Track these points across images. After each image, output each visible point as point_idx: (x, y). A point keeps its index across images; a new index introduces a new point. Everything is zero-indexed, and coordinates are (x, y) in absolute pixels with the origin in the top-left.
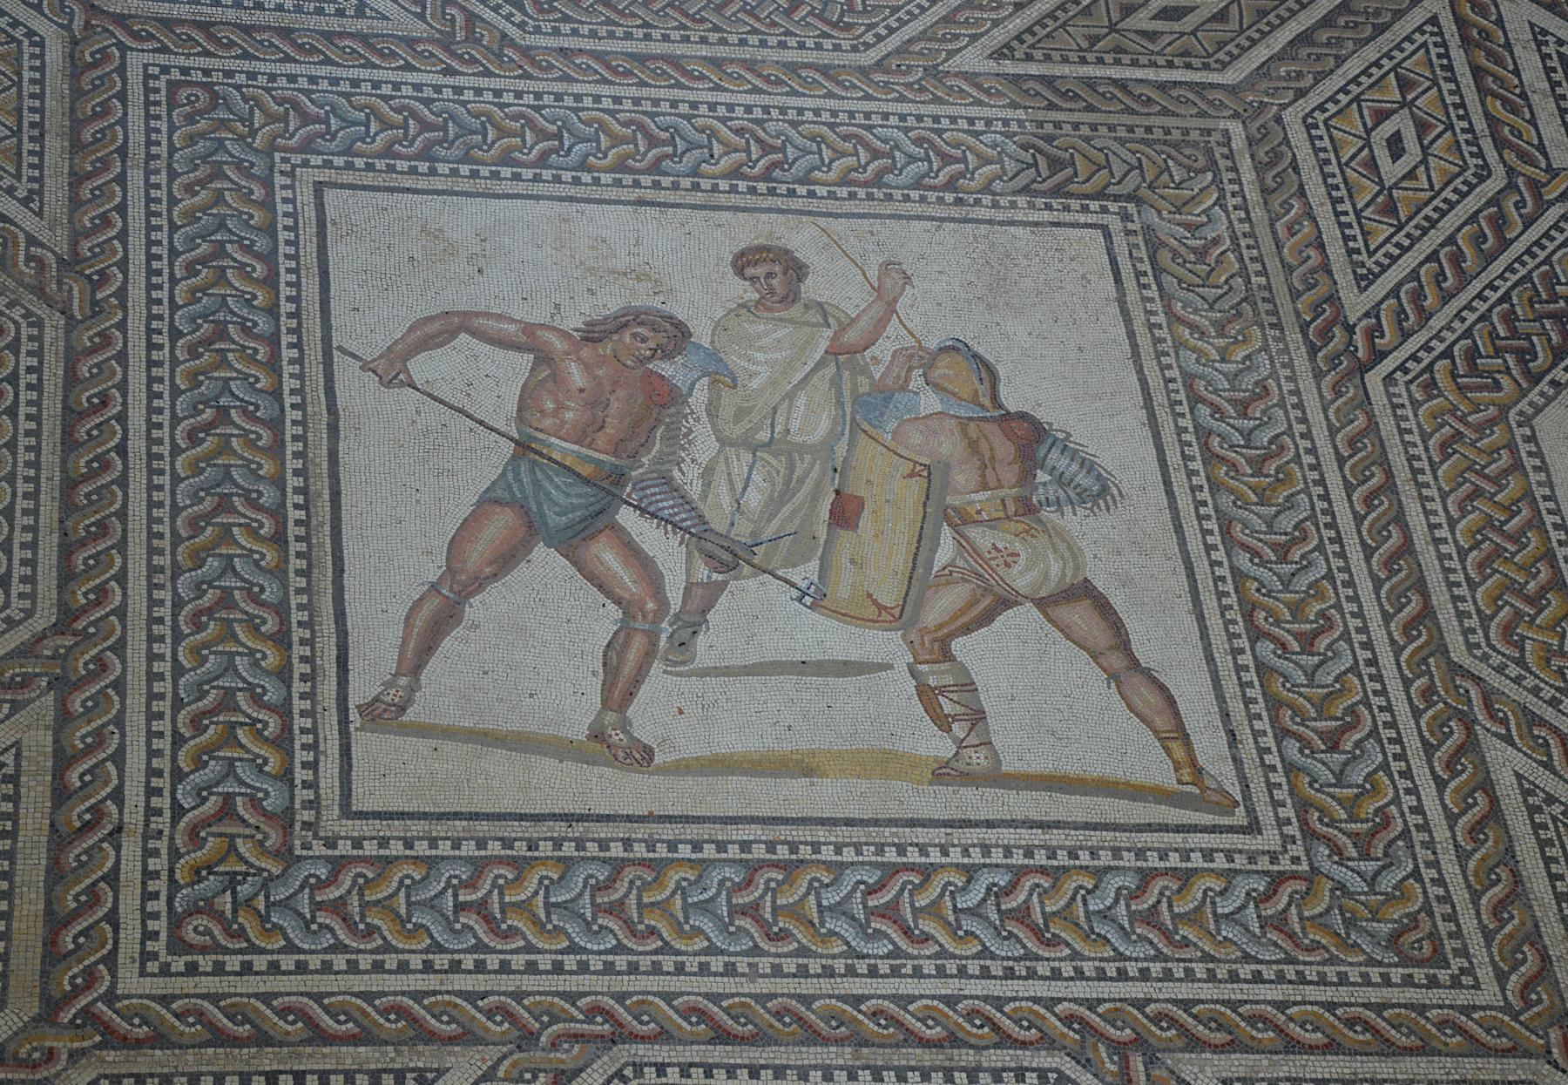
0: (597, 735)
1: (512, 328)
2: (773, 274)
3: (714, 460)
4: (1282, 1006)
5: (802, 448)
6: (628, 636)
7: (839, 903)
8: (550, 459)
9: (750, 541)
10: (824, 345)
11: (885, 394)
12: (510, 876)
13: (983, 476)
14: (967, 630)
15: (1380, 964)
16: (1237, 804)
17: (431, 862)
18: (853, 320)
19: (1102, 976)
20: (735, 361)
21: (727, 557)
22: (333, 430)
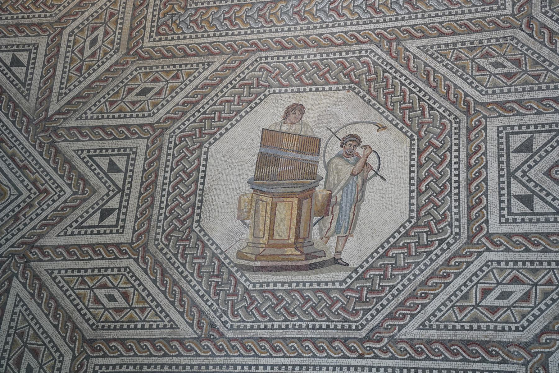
4: (441, 23)
15: (476, 6)
17: (219, 7)
19: (391, 21)
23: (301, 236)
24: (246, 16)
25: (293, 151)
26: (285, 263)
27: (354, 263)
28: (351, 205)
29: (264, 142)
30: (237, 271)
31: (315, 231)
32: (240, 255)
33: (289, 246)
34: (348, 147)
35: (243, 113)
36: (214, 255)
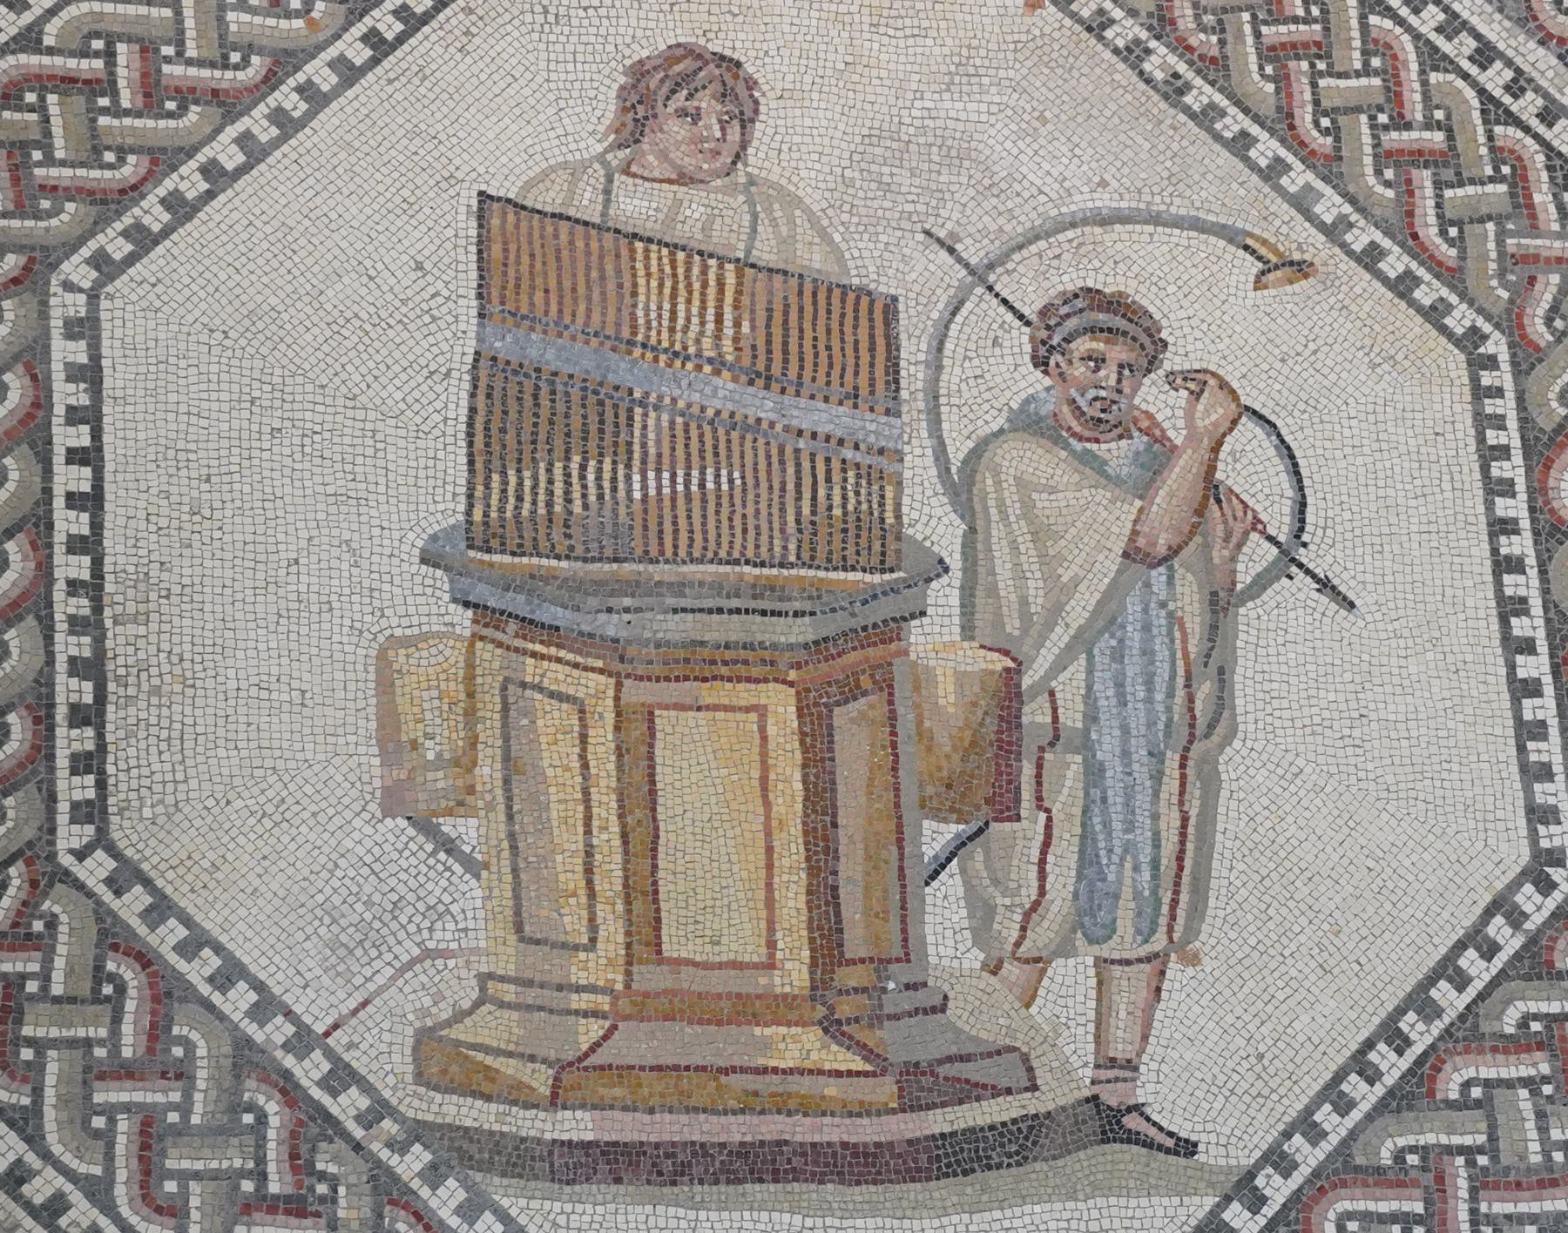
23: (856, 942)
25: (718, 365)
26: (771, 1127)
27: (1231, 1140)
28: (1156, 755)
29: (496, 289)
30: (434, 1176)
31: (944, 913)
32: (441, 1058)
33: (780, 1009)
34: (1080, 371)
35: (318, 72)
36: (245, 1058)
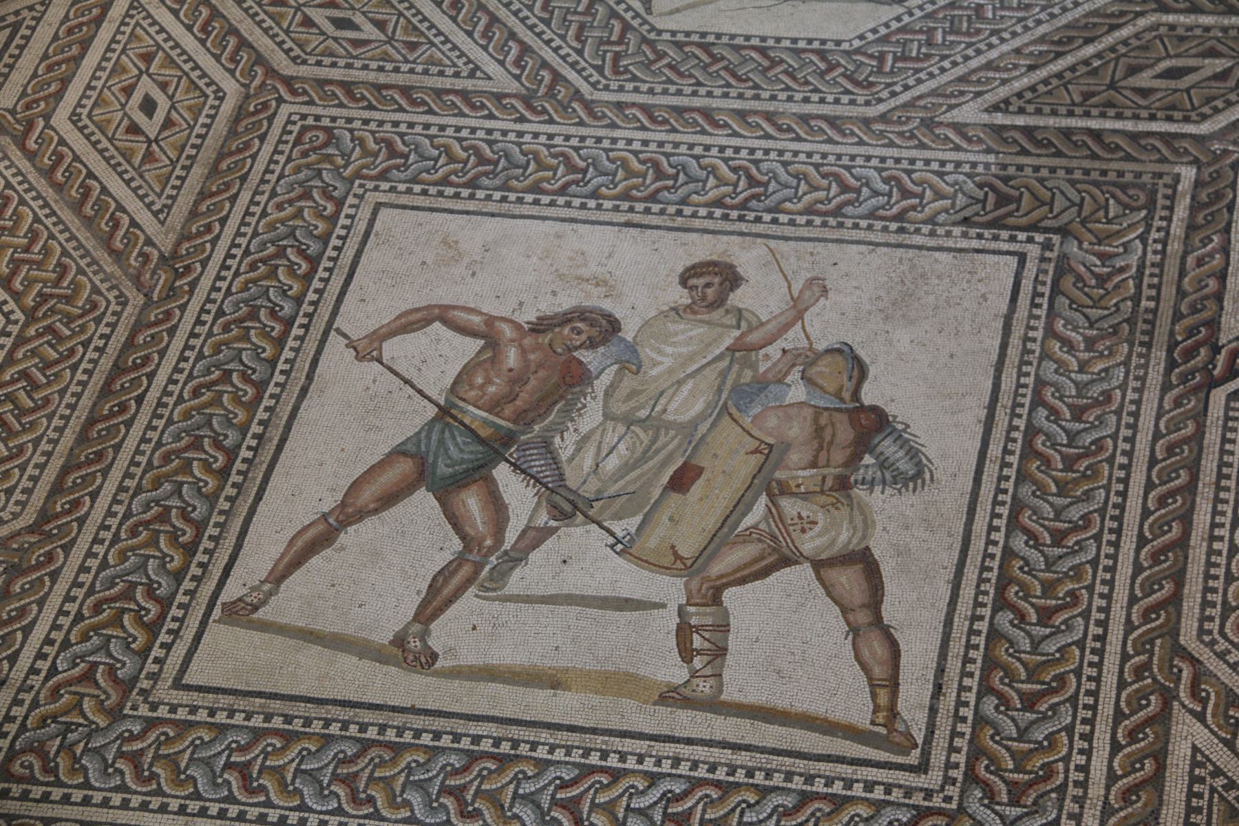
0: (400, 641)
1: (476, 319)
2: (713, 283)
3: (592, 432)
5: (669, 426)
6: (460, 566)
7: (532, 793)
8: (462, 423)
9: (592, 497)
10: (728, 342)
11: (762, 384)
12: (279, 745)
13: (816, 457)
14: (743, 581)
16: (916, 746)
18: (762, 324)
20: (647, 353)
21: (567, 507)
22: (304, 391)
24: (298, 771)
